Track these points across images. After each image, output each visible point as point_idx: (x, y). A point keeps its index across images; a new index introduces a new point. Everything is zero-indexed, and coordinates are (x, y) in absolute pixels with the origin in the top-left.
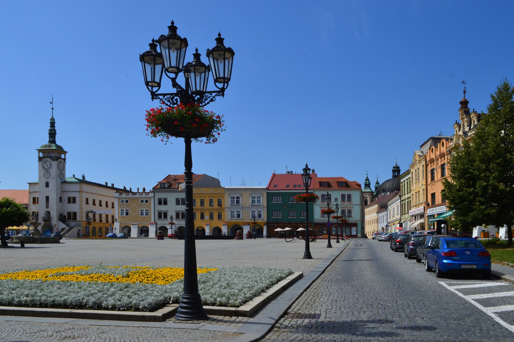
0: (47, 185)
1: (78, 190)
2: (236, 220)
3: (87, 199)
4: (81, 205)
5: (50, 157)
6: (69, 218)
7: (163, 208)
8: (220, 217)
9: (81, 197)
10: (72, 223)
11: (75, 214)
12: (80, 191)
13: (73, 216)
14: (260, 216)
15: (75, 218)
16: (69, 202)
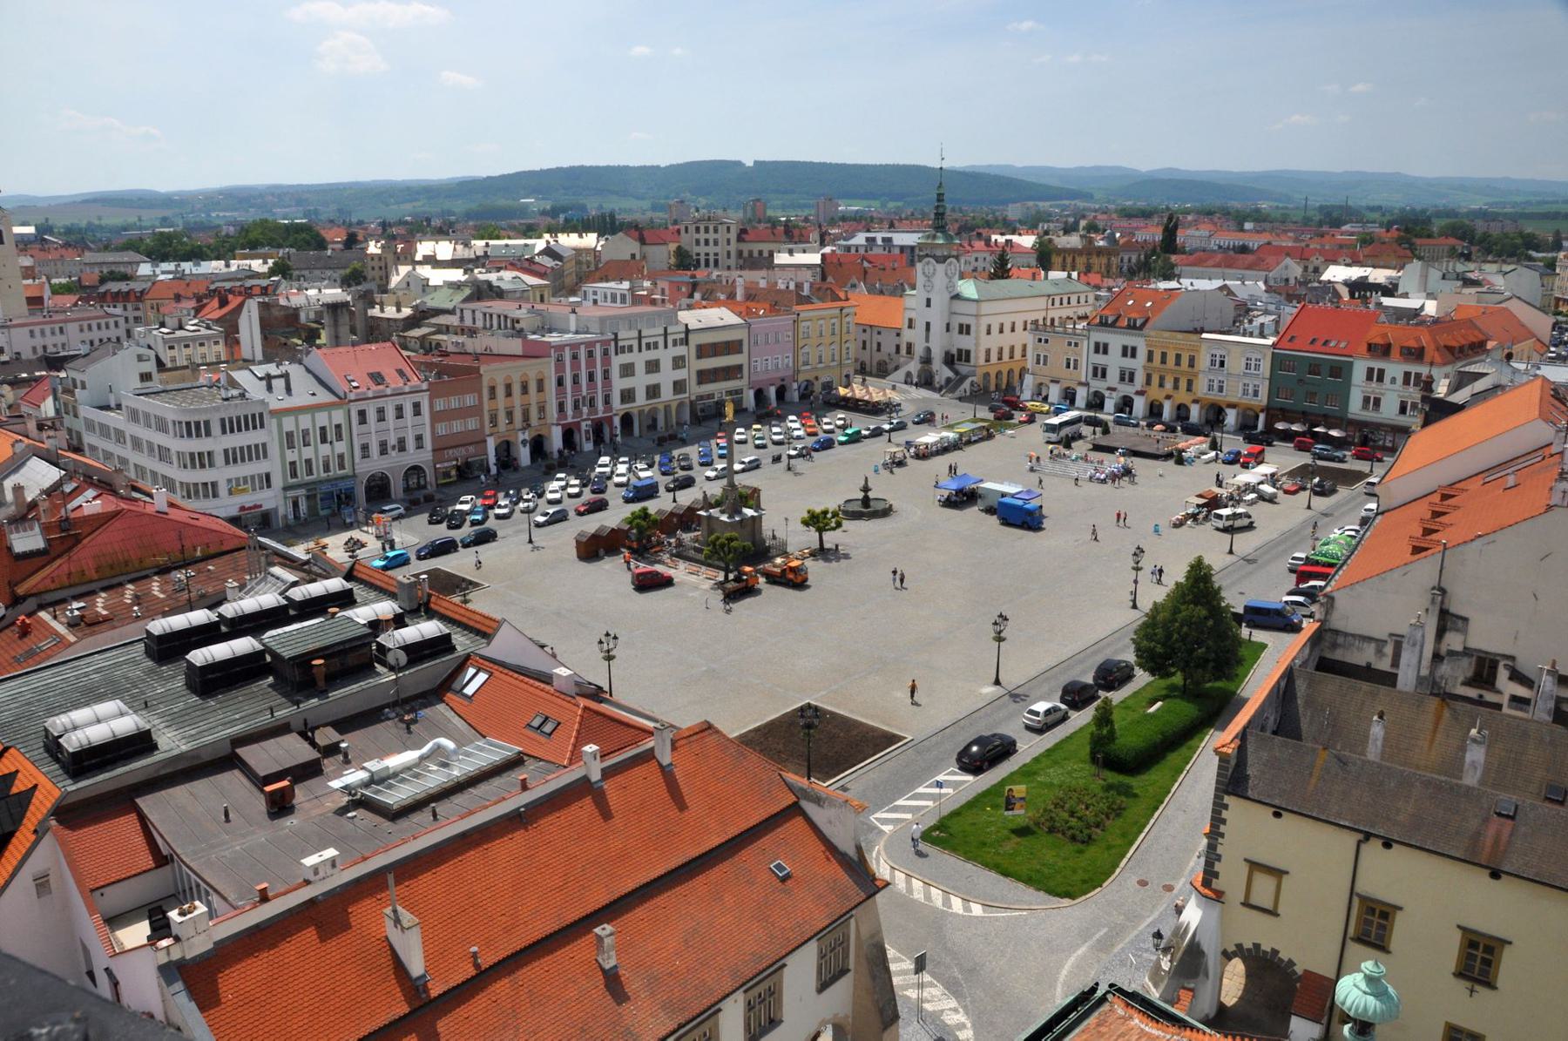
2: (1214, 396)
4: (977, 338)
5: (934, 257)
6: (960, 359)
7: (1100, 359)
8: (1189, 389)
9: (978, 325)
10: (963, 368)
11: (968, 352)
13: (965, 355)
14: (1256, 393)
15: (968, 360)
16: (961, 332)
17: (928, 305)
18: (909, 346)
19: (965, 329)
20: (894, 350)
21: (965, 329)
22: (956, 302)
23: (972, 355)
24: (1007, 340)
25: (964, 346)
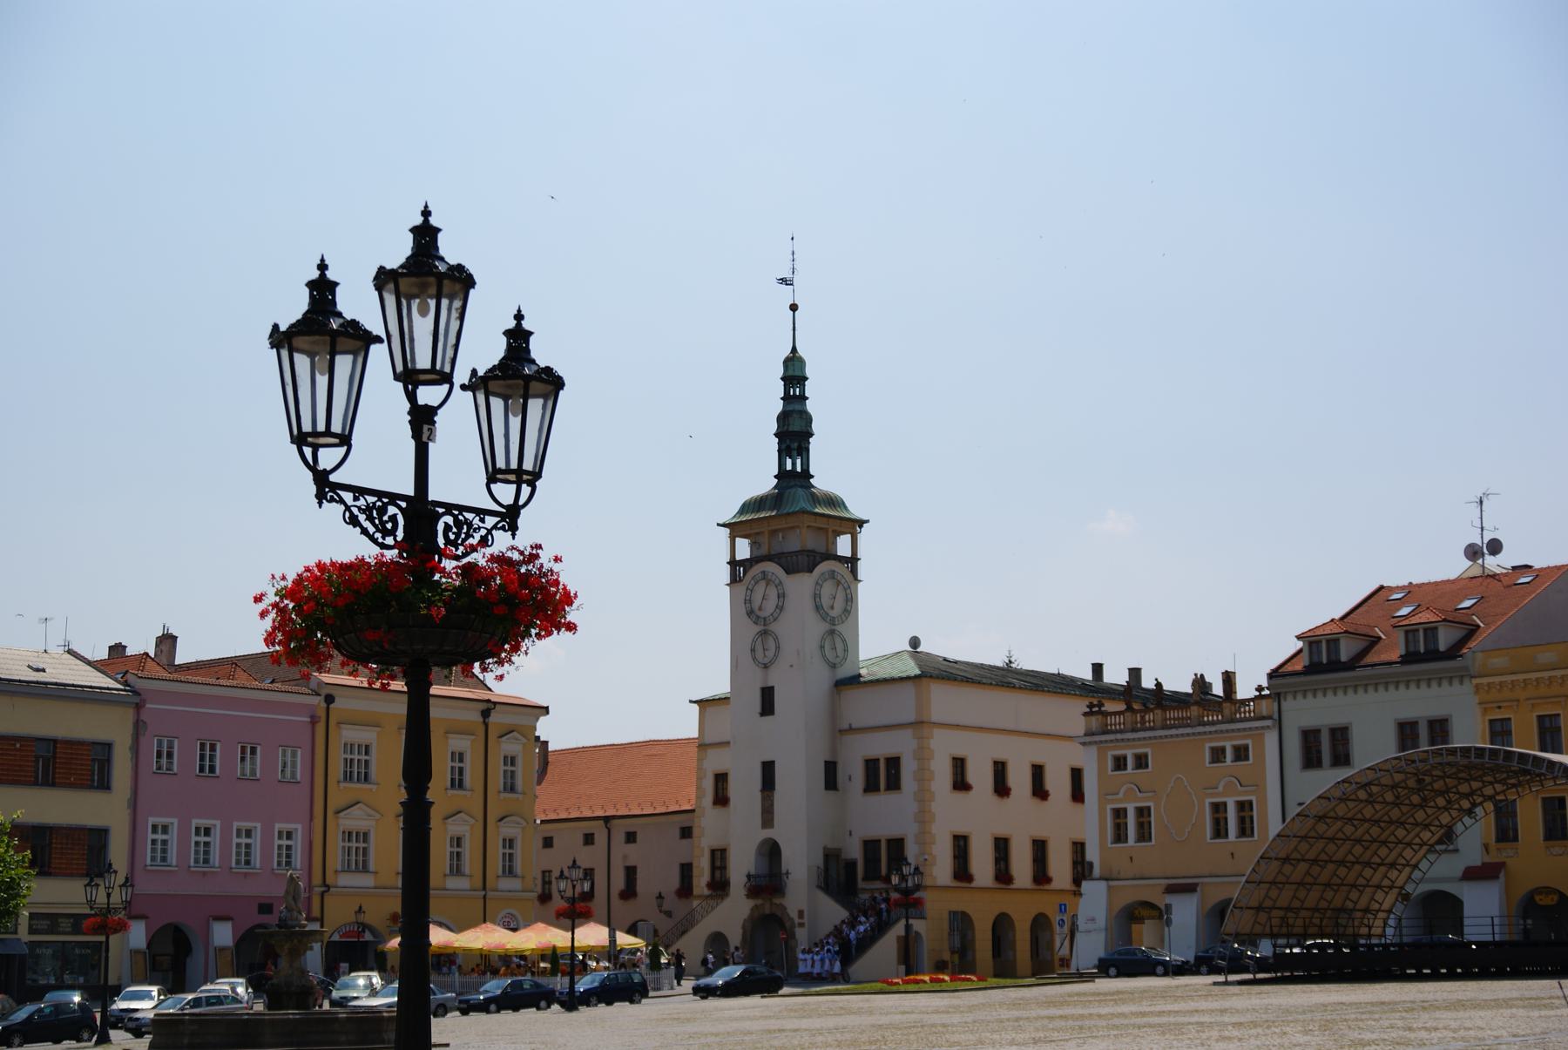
0: (767, 703)
1: (910, 716)
3: (959, 764)
4: (923, 797)
9: (923, 755)
11: (897, 845)
12: (919, 725)
16: (871, 786)
17: (767, 707)
18: (719, 857)
19: (883, 775)
20: (675, 882)
21: (883, 775)
22: (851, 695)
23: (911, 851)
24: (1020, 819)
25: (883, 830)
